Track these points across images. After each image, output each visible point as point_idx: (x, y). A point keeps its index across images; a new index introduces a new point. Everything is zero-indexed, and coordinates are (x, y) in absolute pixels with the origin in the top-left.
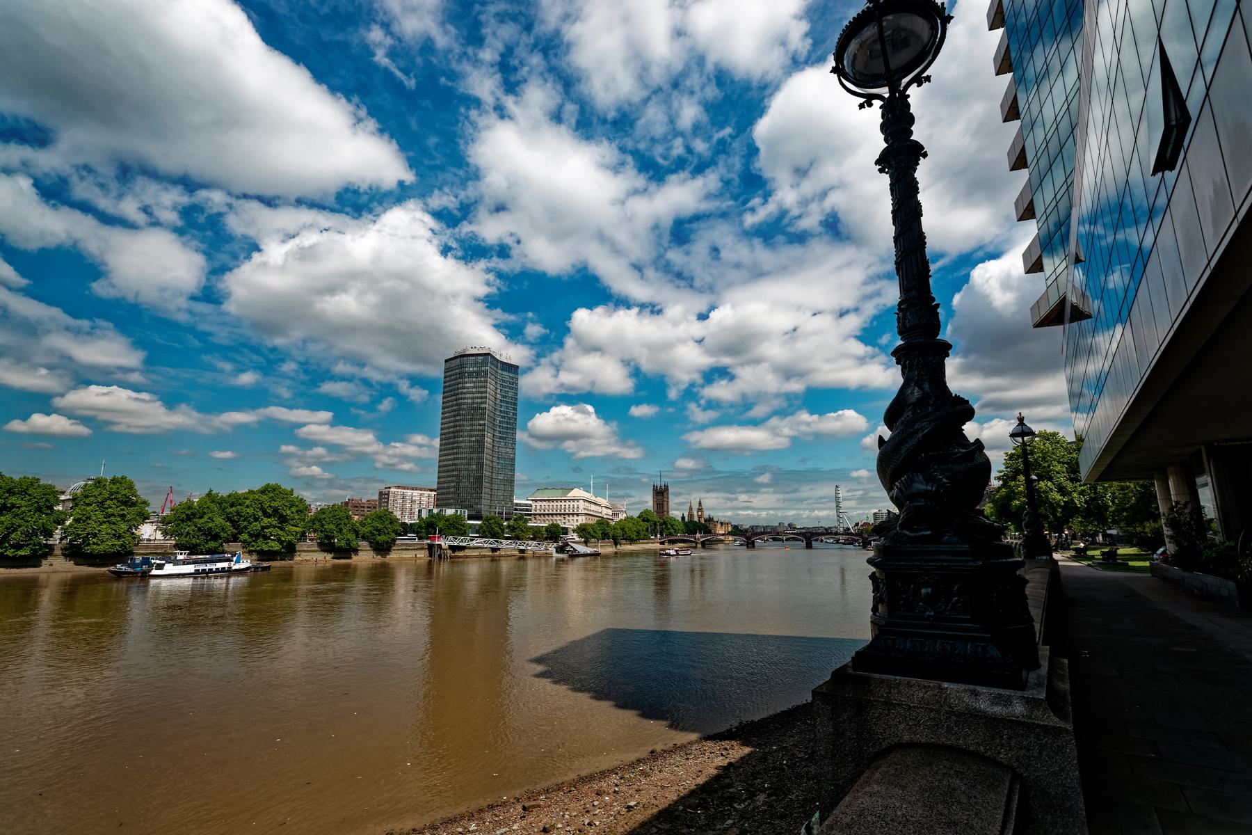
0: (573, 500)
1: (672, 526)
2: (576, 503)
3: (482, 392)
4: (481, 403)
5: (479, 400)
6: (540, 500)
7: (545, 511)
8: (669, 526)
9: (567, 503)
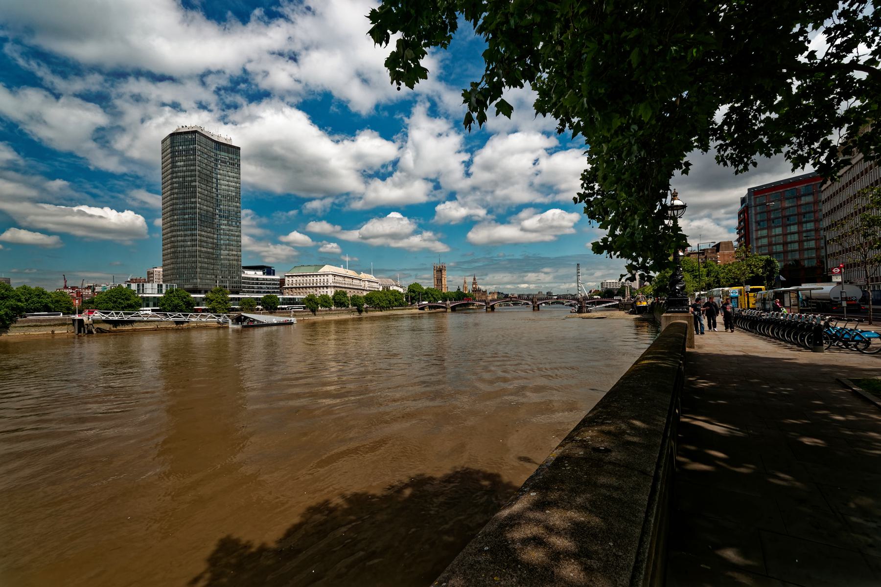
0: (324, 275)
1: (432, 295)
2: (326, 278)
3: (192, 171)
4: (192, 181)
5: (190, 179)
6: (296, 276)
7: (300, 285)
8: (430, 295)
9: (319, 278)
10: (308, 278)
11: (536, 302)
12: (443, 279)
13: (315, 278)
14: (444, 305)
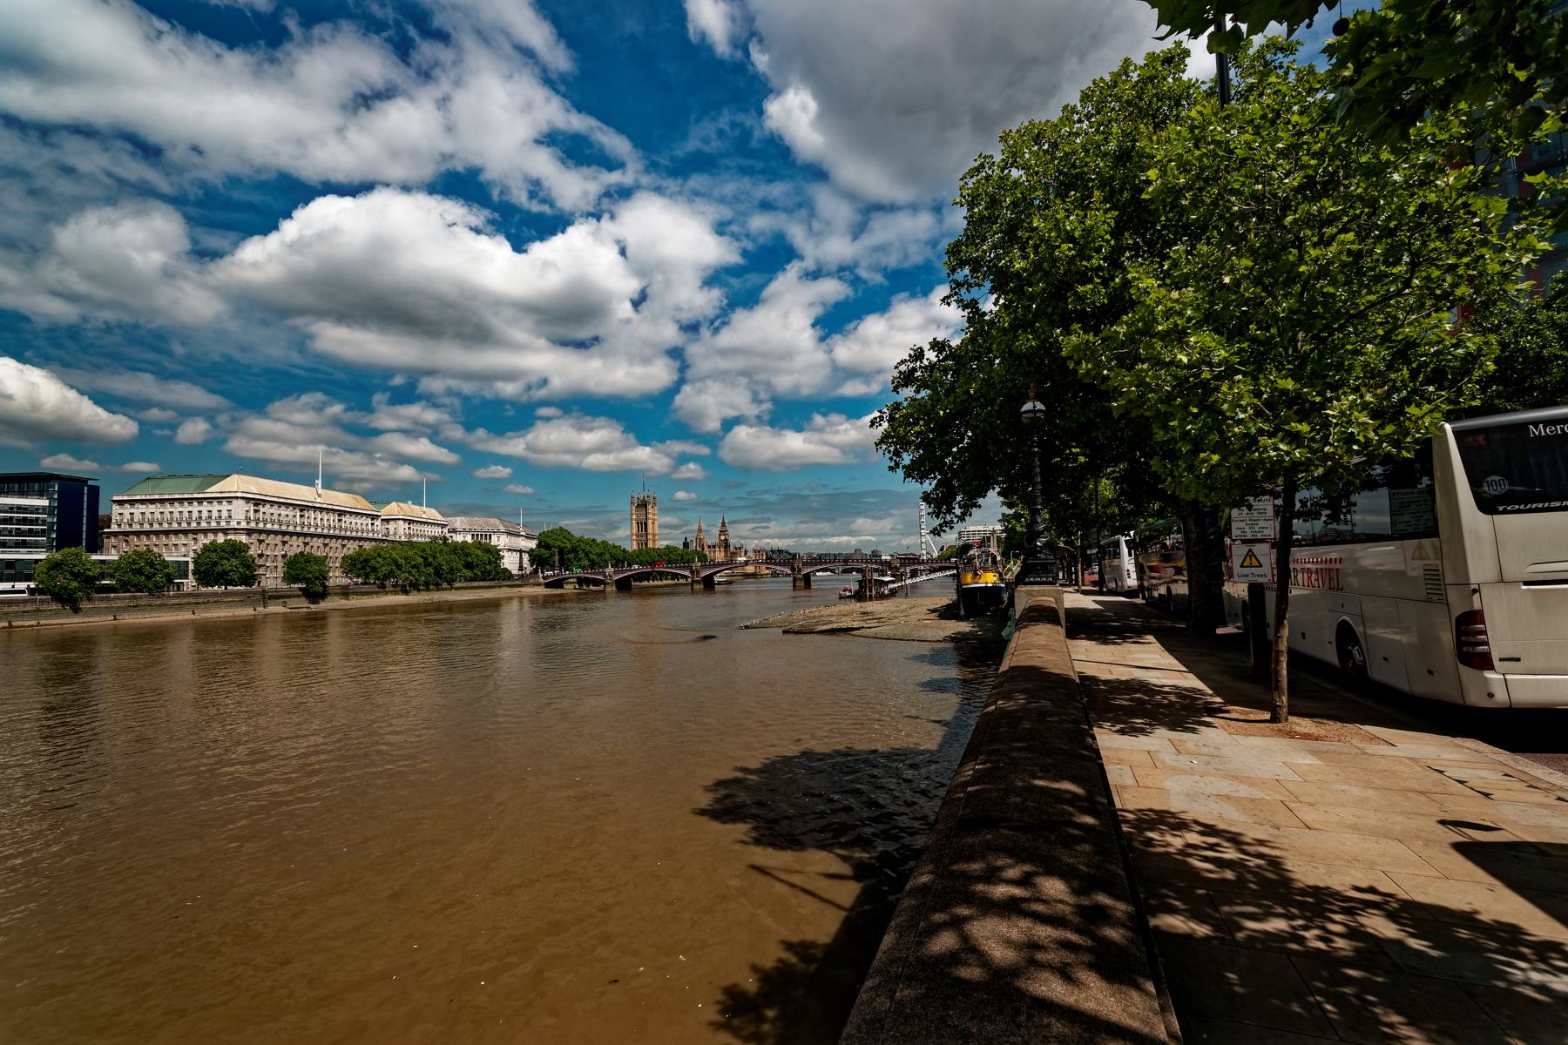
0: (219, 500)
1: (587, 554)
2: (225, 506)
6: (143, 502)
7: (151, 525)
8: (582, 555)
9: (205, 507)
10: (177, 508)
11: (800, 570)
12: (650, 522)
13: (195, 508)
14: (601, 577)
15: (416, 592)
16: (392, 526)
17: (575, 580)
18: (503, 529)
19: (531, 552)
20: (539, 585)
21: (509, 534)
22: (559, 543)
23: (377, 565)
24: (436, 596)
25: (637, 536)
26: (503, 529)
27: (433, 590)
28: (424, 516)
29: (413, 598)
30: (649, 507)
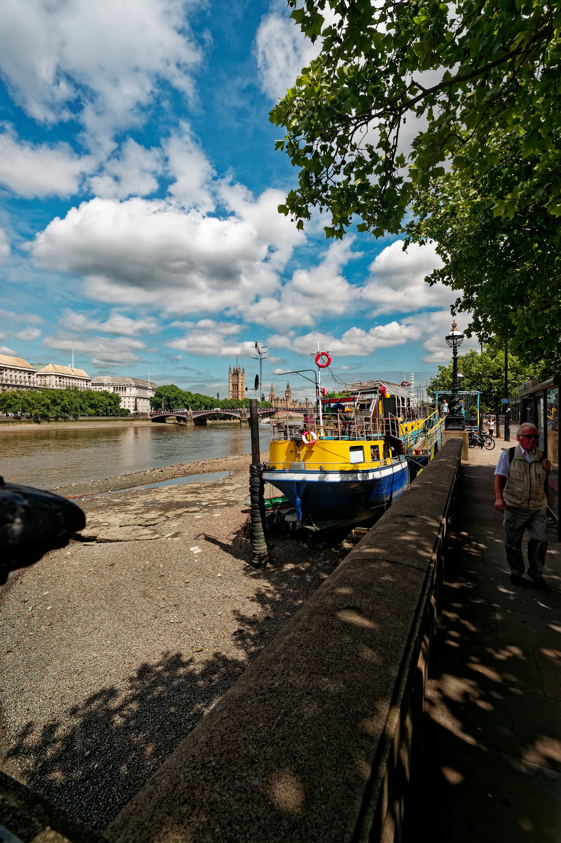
12: (240, 384)
15: (46, 422)
16: (48, 379)
17: (175, 418)
18: (133, 384)
19: (151, 399)
20: (147, 420)
21: (138, 387)
22: (167, 394)
23: (12, 403)
24: (62, 426)
25: (232, 392)
26: (133, 384)
27: (61, 421)
28: (72, 374)
29: (44, 426)
30: (240, 375)
